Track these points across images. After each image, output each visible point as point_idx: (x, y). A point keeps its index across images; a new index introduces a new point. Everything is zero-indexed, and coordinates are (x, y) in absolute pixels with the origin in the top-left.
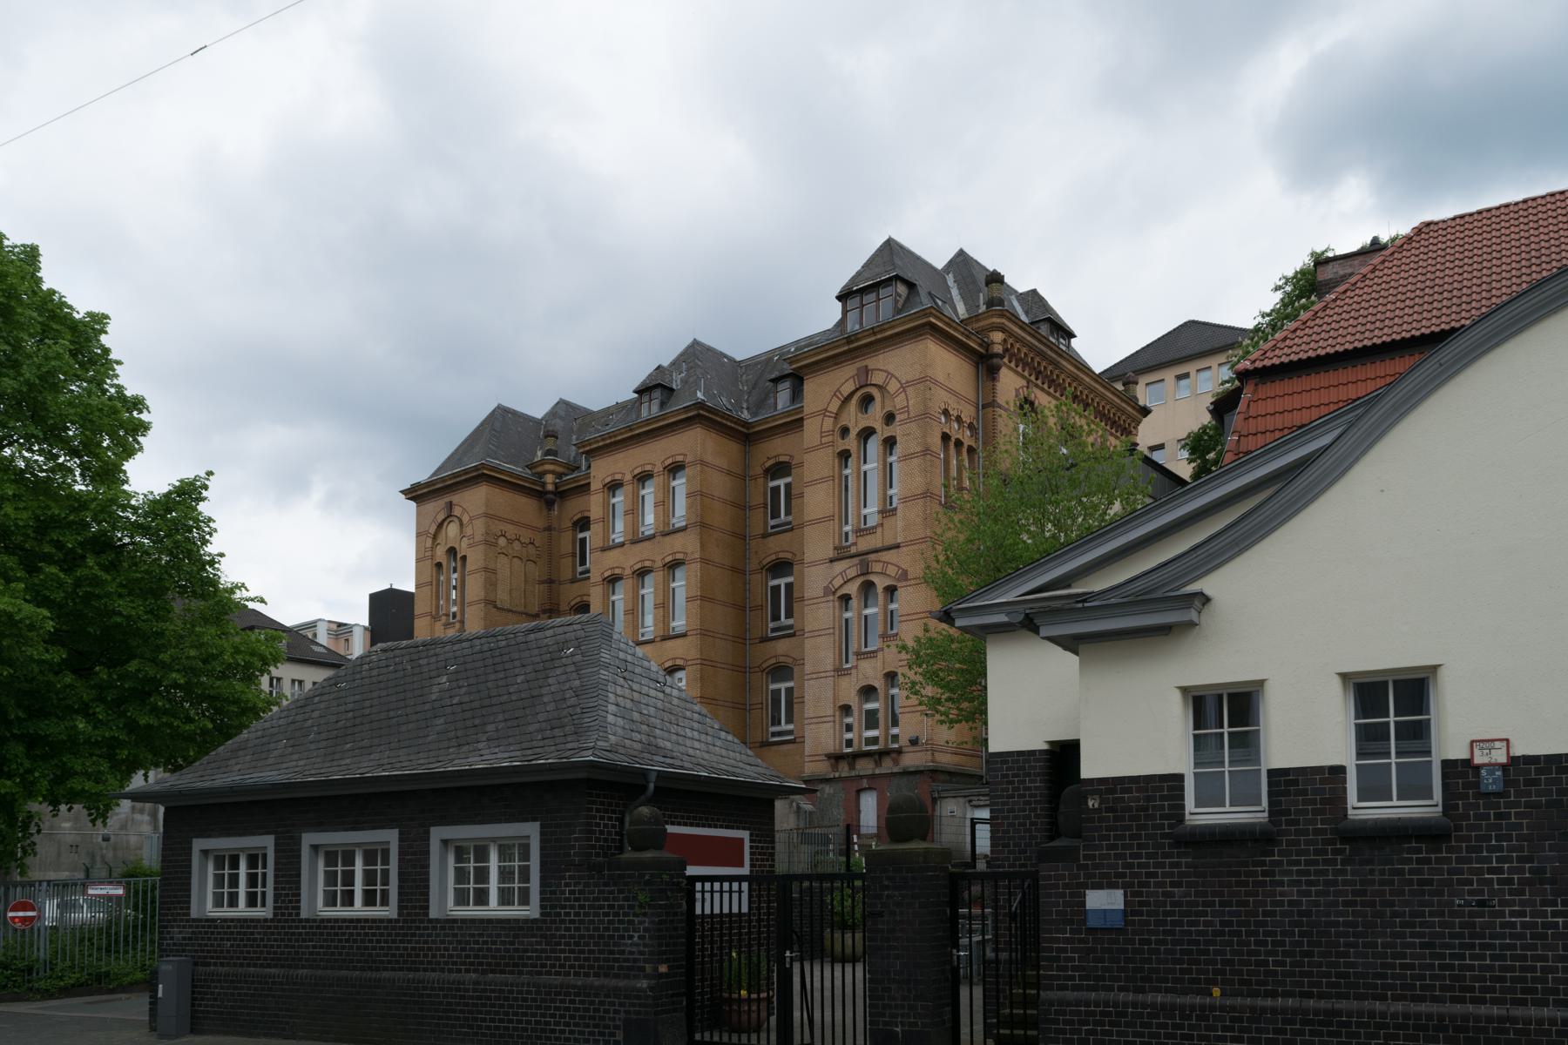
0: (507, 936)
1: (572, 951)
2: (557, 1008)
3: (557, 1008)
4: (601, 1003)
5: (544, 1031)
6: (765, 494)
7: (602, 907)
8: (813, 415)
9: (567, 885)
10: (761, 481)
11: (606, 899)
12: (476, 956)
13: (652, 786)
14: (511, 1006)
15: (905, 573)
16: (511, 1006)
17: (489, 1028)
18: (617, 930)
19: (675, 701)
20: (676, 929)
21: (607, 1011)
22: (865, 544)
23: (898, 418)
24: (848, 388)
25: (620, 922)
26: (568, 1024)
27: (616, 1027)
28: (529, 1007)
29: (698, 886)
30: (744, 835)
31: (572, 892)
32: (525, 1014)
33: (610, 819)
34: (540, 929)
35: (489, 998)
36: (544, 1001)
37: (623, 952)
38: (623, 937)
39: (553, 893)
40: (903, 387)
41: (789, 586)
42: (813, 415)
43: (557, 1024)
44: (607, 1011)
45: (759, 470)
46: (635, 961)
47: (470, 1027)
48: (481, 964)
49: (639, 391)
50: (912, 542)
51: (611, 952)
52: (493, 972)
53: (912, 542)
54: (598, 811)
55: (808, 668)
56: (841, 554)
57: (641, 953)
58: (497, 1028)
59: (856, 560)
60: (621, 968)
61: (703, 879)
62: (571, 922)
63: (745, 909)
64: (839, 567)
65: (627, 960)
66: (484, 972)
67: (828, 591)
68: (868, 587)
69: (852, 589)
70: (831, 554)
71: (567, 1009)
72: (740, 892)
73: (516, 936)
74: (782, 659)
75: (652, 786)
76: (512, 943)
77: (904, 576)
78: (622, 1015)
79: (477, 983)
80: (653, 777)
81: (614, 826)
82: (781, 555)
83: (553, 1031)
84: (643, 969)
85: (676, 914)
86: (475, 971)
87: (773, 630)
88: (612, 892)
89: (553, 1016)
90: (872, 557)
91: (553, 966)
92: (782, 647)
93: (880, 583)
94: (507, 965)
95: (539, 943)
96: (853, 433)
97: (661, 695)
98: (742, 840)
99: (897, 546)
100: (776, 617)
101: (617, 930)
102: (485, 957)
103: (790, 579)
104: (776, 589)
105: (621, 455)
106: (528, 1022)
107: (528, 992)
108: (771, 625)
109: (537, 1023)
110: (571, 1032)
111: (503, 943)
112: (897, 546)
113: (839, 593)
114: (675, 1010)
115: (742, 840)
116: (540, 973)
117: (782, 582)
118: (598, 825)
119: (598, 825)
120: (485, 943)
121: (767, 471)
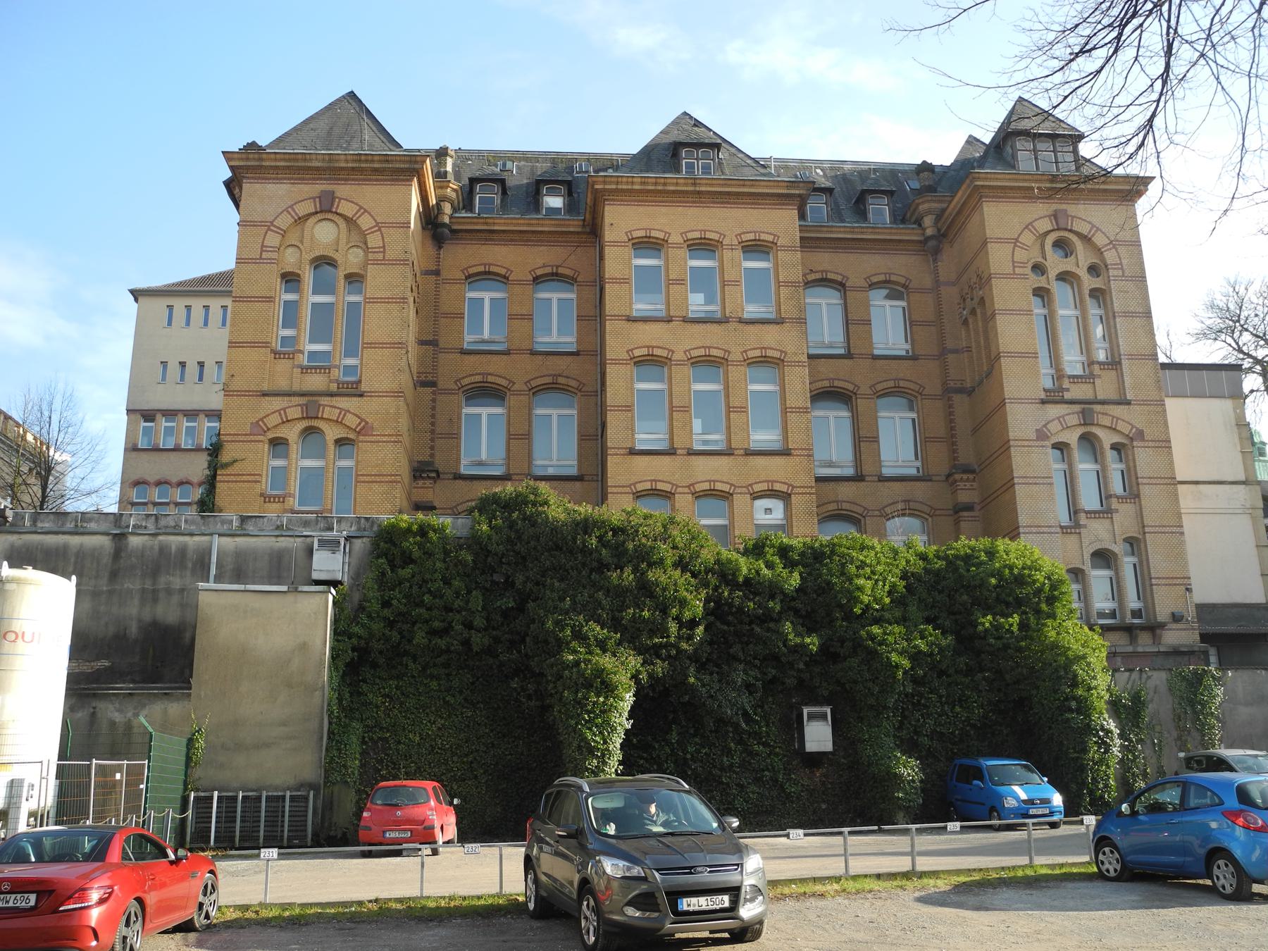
22: (1077, 392)
50: (1145, 403)
53: (1145, 403)
56: (1053, 397)
59: (1077, 408)
64: (1054, 411)
67: (1041, 435)
68: (1088, 440)
69: (1072, 438)
70: (1043, 395)
74: (845, 506)
77: (1140, 434)
90: (1098, 408)
93: (1107, 439)
96: (1052, 274)
99: (1128, 403)
105: (664, 210)
112: (1128, 403)
113: (1054, 440)
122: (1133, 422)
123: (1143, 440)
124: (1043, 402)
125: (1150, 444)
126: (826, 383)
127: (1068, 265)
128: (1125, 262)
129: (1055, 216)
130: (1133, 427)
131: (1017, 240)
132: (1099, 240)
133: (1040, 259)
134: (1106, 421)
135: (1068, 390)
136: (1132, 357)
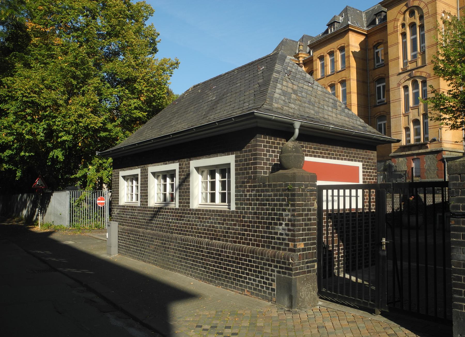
0: (221, 220)
1: (250, 231)
2: (243, 264)
3: (243, 264)
4: (265, 264)
5: (236, 276)
6: (374, 55)
7: (265, 205)
8: (391, 21)
9: (248, 191)
10: (372, 50)
11: (267, 200)
12: (208, 230)
13: (297, 132)
14: (222, 260)
15: (430, 75)
16: (222, 260)
17: (212, 270)
18: (273, 219)
19: (319, 93)
20: (310, 220)
21: (267, 269)
23: (425, 17)
24: (405, 8)
25: (275, 214)
26: (248, 274)
27: (273, 280)
28: (230, 261)
29: (324, 192)
30: (359, 165)
31: (250, 195)
32: (228, 265)
33: (273, 152)
34: (235, 216)
35: (212, 253)
36: (236, 258)
37: (276, 233)
38: (276, 224)
39: (241, 196)
40: (426, 5)
41: (384, 87)
42: (391, 21)
43: (243, 273)
44: (267, 269)
45: (371, 47)
46: (284, 239)
47: (205, 268)
48: (210, 234)
49: (328, 25)
51: (271, 233)
52: (215, 239)
54: (265, 146)
55: (392, 114)
57: (287, 235)
58: (216, 271)
60: (276, 243)
61: (327, 187)
62: (250, 213)
63: (360, 206)
64: (402, 76)
65: (279, 239)
66: (212, 239)
71: (247, 265)
72: (357, 196)
73: (225, 220)
74: (382, 113)
75: (297, 132)
76: (223, 224)
78: (276, 274)
79: (208, 244)
80: (297, 125)
81: (276, 156)
82: (380, 76)
83: (241, 277)
84: (287, 245)
85: (309, 210)
86: (208, 238)
87: (379, 103)
88: (270, 196)
89: (241, 268)
91: (241, 239)
92: (382, 108)
94: (221, 236)
95: (235, 225)
97: (311, 89)
98: (358, 168)
100: (379, 98)
101: (273, 219)
102: (212, 231)
103: (384, 84)
104: (379, 88)
106: (230, 270)
107: (230, 253)
108: (378, 101)
109: (234, 271)
110: (250, 279)
111: (219, 223)
114: (309, 272)
115: (358, 168)
116: (235, 242)
117: (381, 85)
118: (265, 155)
119: (265, 155)
120: (212, 223)
121: (374, 46)
122: (427, 72)
123: (430, 77)
124: (400, 74)
125: (433, 78)
126: (378, 76)
127: (412, 20)
128: (430, 10)
129: (406, 5)
130: (427, 73)
131: (395, 19)
132: (421, 6)
133: (404, 22)
134: (418, 74)
135: (408, 66)
136: (429, 47)
